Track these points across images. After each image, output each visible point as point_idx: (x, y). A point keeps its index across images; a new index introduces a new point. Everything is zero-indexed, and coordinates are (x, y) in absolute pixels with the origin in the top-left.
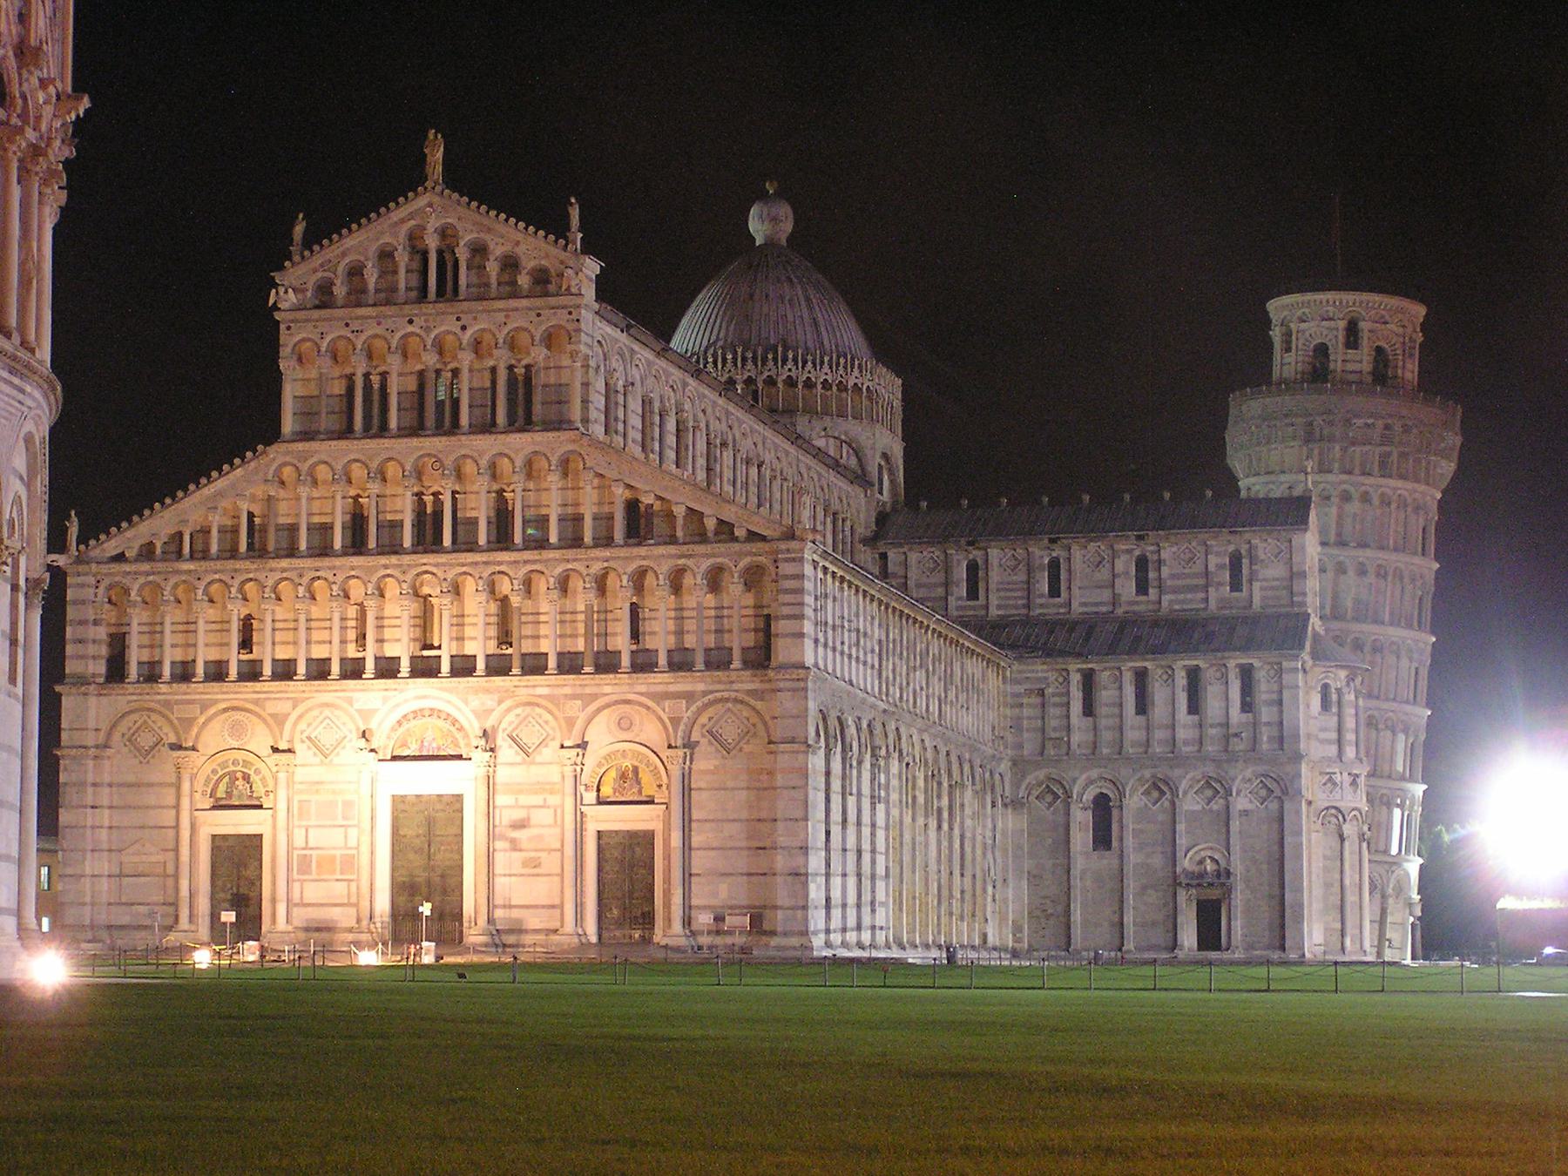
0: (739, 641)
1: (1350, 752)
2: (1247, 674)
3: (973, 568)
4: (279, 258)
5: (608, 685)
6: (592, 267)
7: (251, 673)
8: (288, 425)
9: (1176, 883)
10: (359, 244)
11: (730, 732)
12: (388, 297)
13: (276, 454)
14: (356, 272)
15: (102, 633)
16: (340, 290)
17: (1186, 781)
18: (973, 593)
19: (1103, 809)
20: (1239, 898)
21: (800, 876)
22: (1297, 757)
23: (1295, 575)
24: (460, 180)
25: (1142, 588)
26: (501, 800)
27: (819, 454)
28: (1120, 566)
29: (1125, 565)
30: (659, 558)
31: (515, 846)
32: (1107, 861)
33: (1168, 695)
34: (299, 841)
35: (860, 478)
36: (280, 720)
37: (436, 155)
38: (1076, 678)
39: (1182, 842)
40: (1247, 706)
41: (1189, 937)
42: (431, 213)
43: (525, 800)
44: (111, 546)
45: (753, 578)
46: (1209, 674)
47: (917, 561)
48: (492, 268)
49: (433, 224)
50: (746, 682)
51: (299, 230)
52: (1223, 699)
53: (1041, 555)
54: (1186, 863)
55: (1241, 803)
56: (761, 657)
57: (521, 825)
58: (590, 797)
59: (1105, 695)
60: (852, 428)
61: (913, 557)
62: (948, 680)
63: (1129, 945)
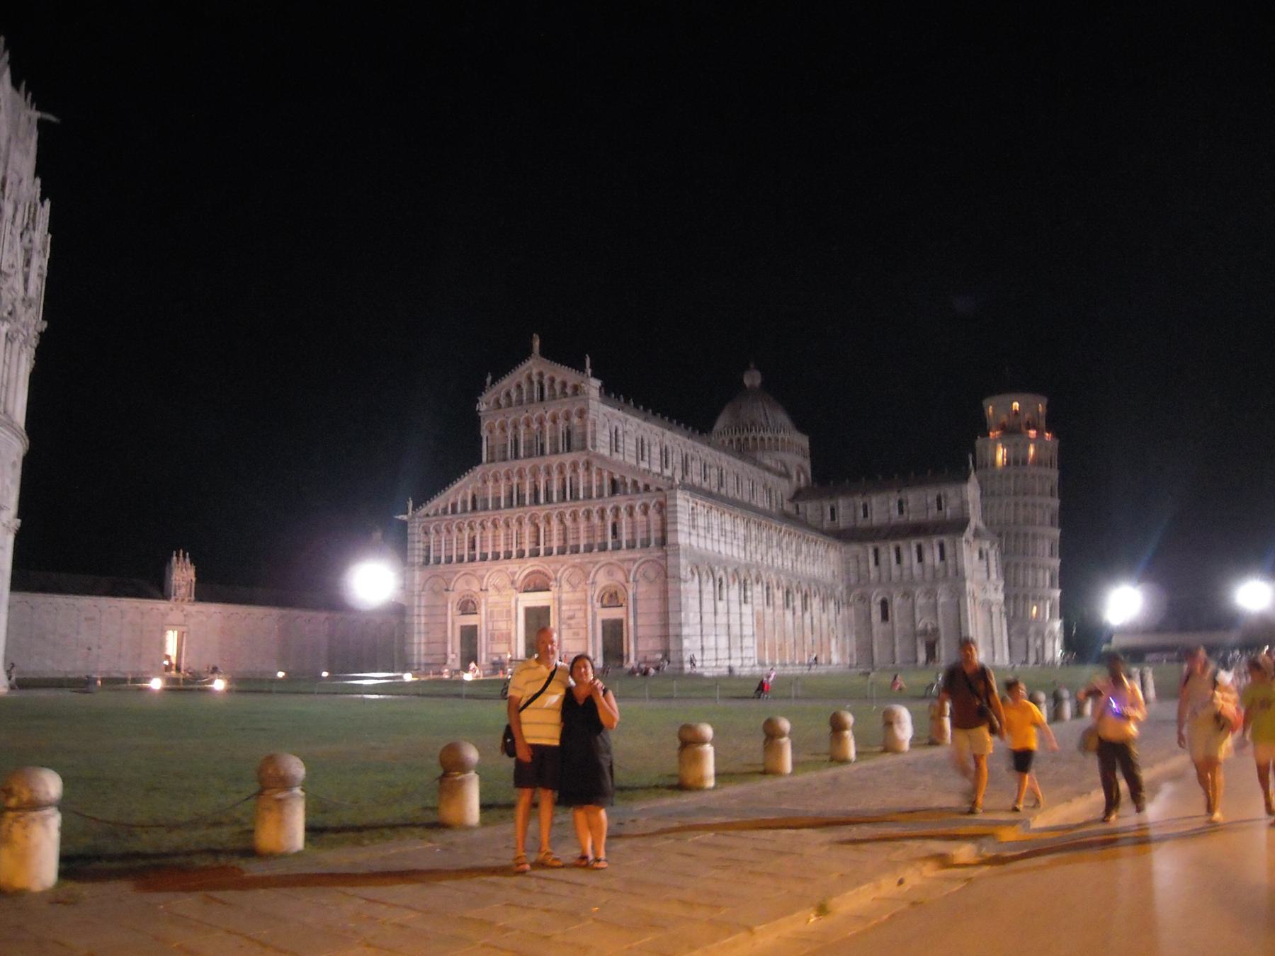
0: (654, 535)
1: (994, 576)
2: (942, 547)
3: (833, 510)
4: (481, 389)
5: (603, 558)
6: (596, 383)
7: (472, 559)
8: (484, 459)
9: (915, 635)
10: (508, 382)
11: (652, 574)
12: (520, 402)
13: (479, 470)
14: (508, 394)
15: (422, 546)
16: (503, 402)
17: (919, 592)
18: (833, 518)
19: (885, 605)
20: (942, 640)
21: (679, 637)
22: (964, 580)
23: (964, 504)
24: (546, 353)
25: (901, 511)
26: (564, 608)
27: (768, 469)
28: (891, 504)
29: (893, 503)
30: (622, 501)
31: (570, 627)
32: (888, 626)
33: (910, 556)
34: (490, 627)
35: (787, 475)
36: (482, 577)
37: (537, 344)
38: (871, 551)
39: (918, 617)
40: (942, 557)
41: (922, 656)
42: (534, 366)
43: (573, 607)
44: (424, 510)
45: (662, 507)
46: (925, 546)
47: (809, 509)
48: (558, 387)
49: (535, 372)
50: (656, 553)
51: (489, 379)
52: (932, 556)
53: (859, 501)
54: (920, 626)
55: (942, 599)
56: (663, 542)
57: (571, 618)
58: (598, 605)
59: (883, 557)
60: (782, 455)
61: (809, 505)
62: (798, 553)
63: (898, 662)
